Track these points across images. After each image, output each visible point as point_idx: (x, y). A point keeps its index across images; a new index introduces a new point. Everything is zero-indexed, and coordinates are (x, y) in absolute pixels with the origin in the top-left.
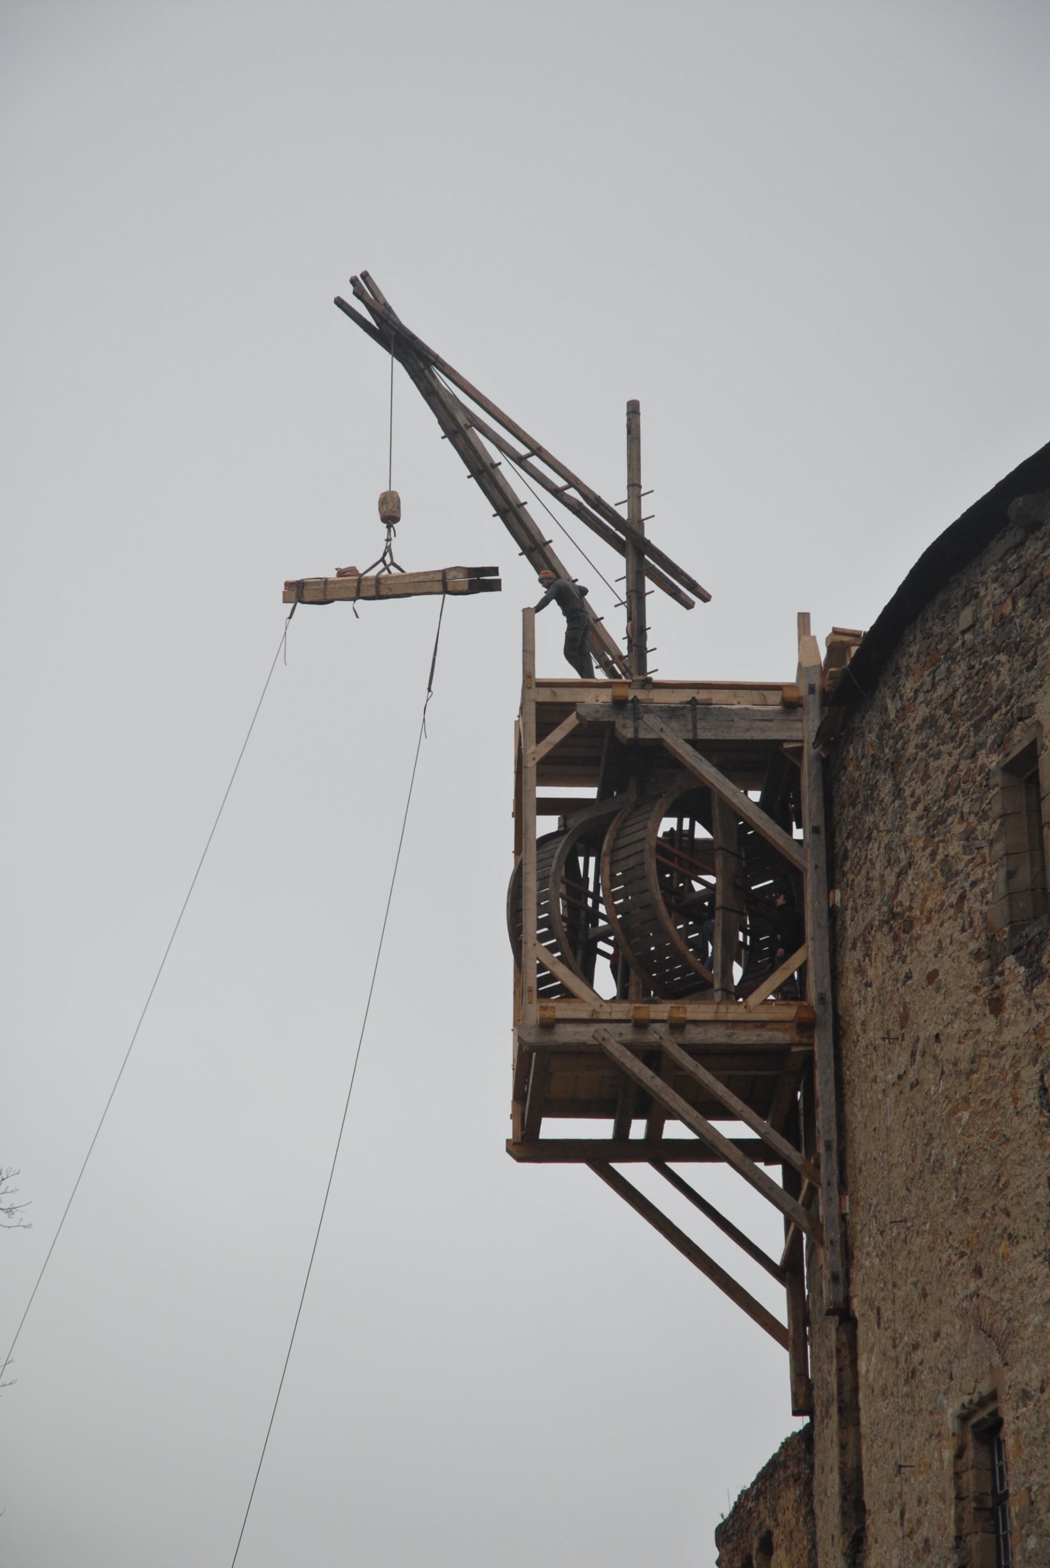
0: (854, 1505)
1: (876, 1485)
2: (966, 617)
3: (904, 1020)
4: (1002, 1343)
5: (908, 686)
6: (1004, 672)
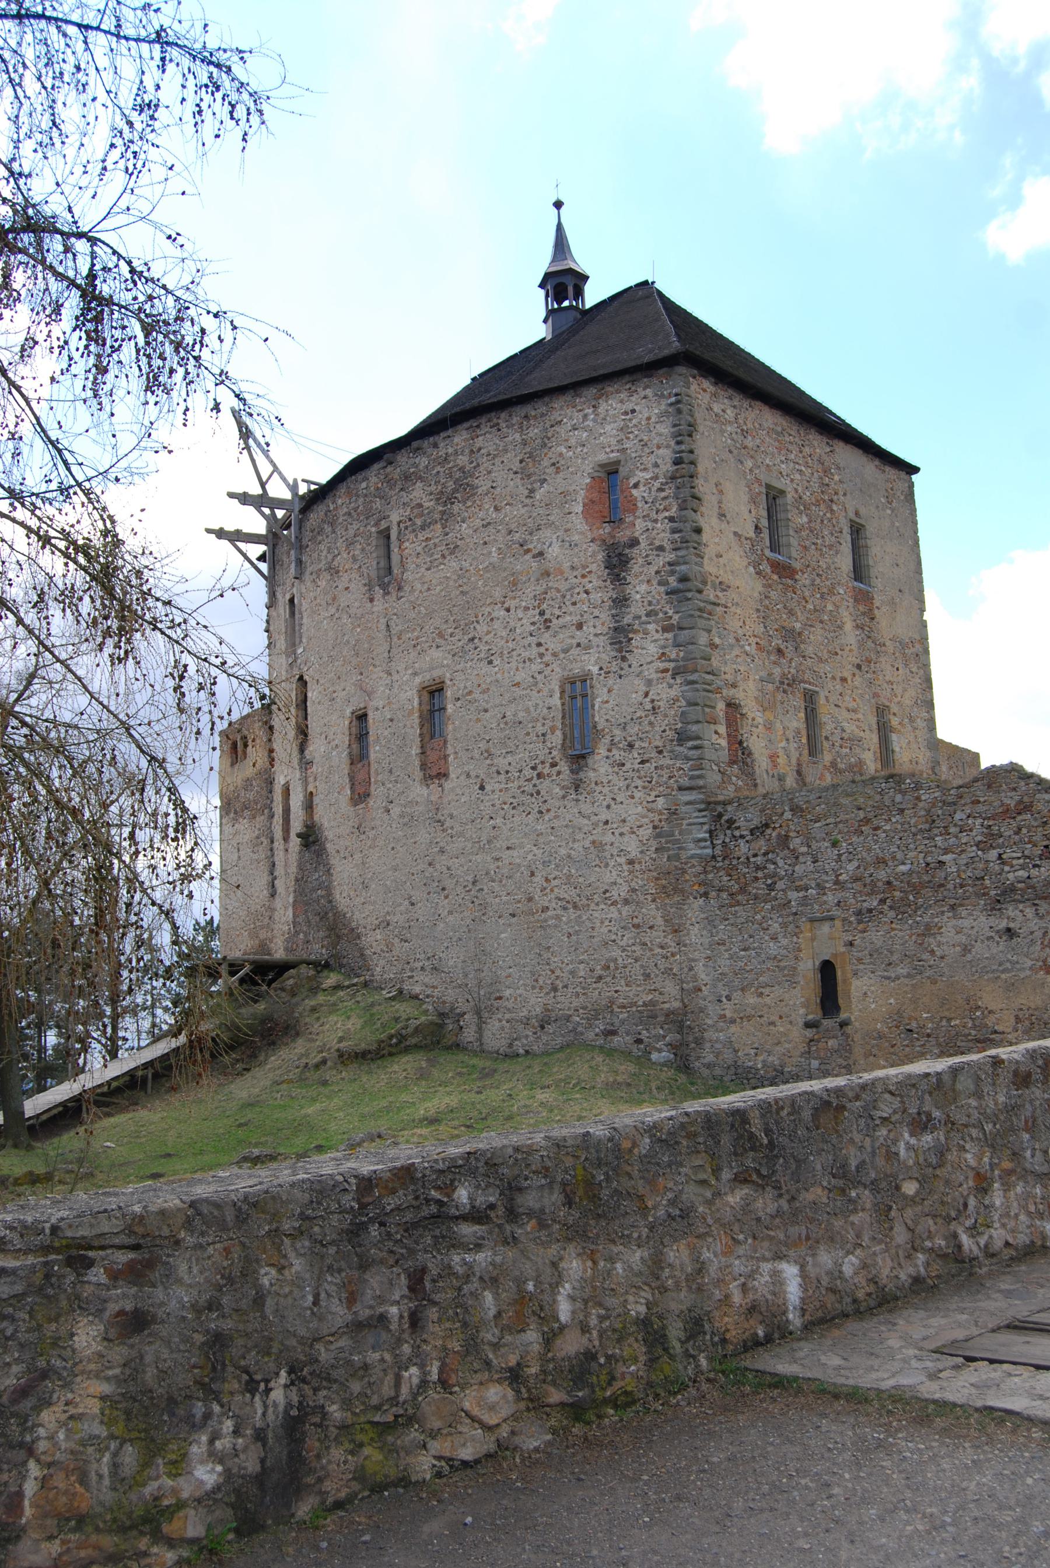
0: (303, 732)
2: (364, 485)
3: (334, 599)
4: (370, 694)
5: (340, 502)
6: (378, 504)
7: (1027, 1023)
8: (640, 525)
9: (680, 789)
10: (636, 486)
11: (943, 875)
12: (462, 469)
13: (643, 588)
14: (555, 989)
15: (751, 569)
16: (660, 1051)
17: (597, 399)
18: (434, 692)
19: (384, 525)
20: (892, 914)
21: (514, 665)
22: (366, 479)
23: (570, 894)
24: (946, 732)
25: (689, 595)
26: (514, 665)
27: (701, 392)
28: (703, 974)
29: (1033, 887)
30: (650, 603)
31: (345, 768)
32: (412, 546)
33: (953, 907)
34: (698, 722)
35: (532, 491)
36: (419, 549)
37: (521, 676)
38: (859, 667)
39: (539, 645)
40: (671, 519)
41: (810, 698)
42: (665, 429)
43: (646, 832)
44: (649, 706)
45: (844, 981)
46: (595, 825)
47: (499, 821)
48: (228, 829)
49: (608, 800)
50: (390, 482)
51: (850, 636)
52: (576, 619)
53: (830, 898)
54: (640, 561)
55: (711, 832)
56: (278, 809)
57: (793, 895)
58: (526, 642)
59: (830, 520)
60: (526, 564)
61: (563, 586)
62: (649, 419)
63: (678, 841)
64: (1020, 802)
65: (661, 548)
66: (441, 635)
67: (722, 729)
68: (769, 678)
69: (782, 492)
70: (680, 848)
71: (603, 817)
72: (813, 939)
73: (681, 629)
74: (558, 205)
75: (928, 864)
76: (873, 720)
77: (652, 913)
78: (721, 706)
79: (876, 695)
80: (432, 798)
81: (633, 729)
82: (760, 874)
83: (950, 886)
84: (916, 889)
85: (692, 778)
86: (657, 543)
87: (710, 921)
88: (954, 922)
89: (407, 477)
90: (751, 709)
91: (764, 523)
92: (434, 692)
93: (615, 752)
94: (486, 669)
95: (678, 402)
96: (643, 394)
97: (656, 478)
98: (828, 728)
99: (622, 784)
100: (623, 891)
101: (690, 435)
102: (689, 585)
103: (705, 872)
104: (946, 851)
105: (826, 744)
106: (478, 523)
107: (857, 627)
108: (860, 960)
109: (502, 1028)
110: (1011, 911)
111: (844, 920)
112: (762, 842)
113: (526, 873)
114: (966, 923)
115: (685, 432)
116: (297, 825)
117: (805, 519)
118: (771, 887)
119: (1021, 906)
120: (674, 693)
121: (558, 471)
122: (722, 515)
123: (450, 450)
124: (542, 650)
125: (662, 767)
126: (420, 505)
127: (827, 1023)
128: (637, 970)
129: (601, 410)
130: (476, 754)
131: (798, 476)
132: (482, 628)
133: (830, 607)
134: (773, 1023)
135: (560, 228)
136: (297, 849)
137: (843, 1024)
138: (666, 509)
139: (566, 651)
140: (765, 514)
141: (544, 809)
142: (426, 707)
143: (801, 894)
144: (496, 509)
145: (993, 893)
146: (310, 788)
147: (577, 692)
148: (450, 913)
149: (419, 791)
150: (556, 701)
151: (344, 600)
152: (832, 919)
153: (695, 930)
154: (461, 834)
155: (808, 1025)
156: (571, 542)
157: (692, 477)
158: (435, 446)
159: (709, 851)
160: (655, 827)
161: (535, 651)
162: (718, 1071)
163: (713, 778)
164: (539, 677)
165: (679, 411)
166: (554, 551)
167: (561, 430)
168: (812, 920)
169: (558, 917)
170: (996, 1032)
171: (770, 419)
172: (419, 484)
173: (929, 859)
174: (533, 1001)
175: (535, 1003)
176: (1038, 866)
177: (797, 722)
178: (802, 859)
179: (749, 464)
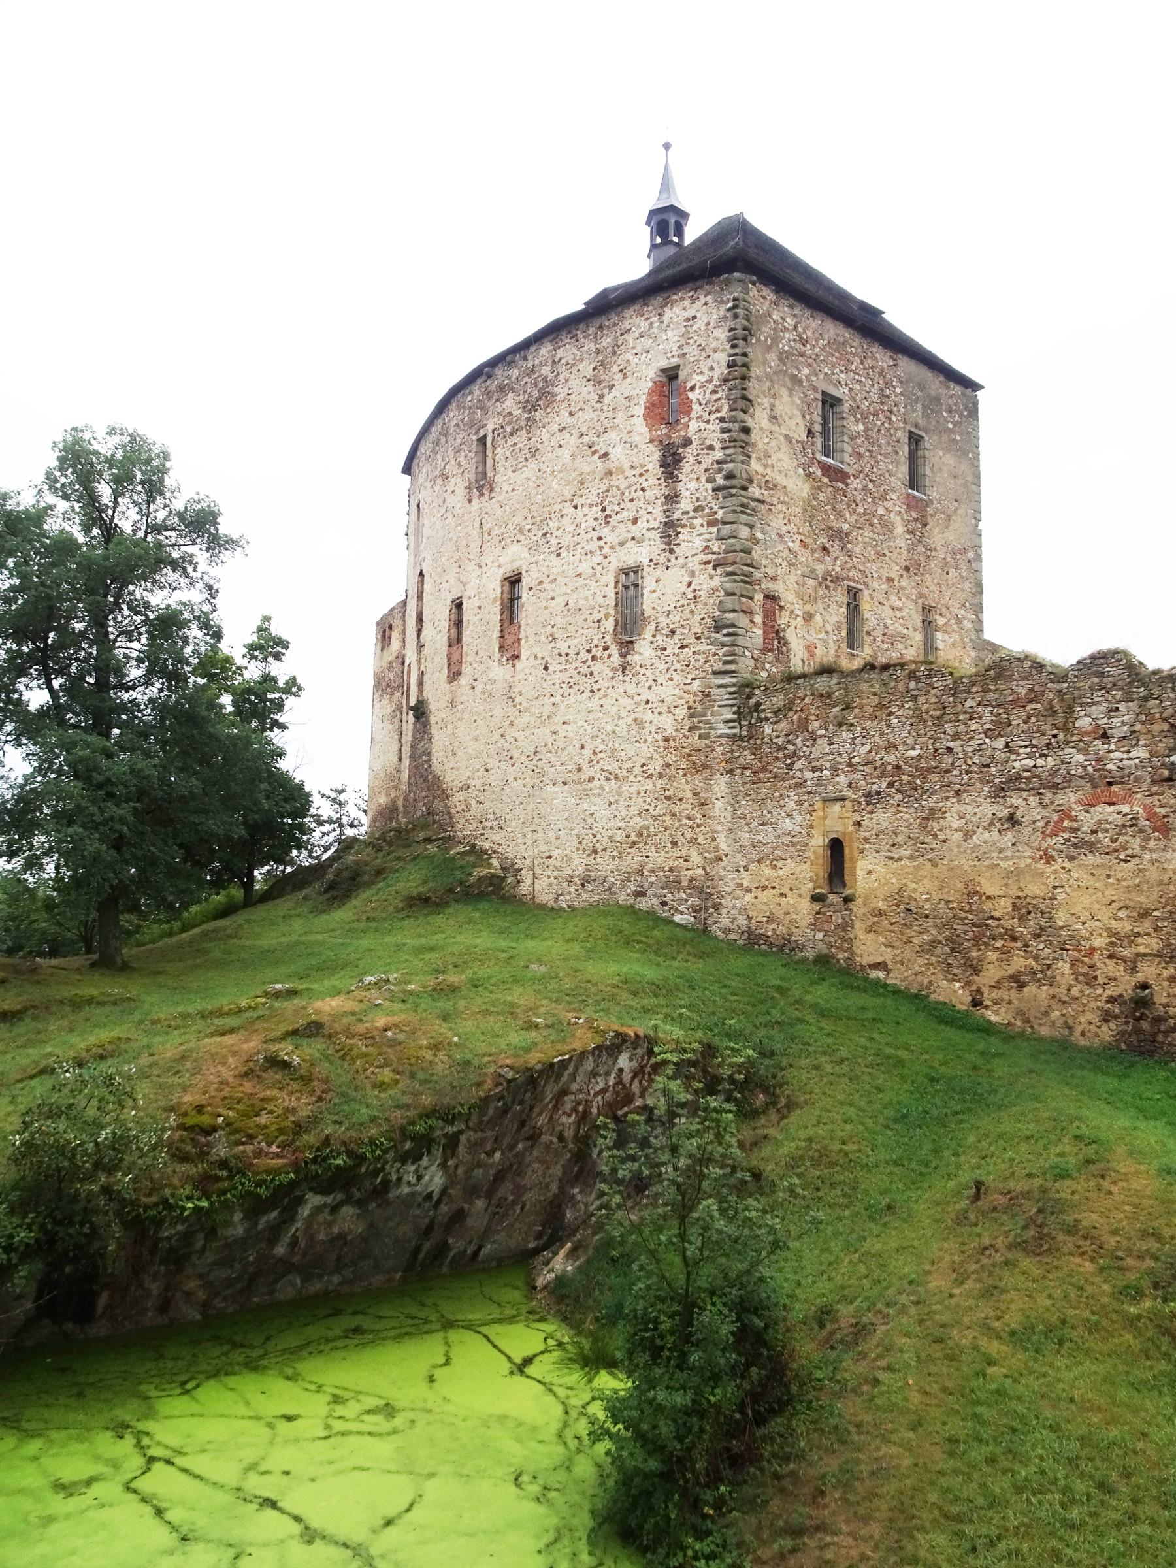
0: (420, 619)
7: (1024, 911)
8: (694, 425)
9: (714, 673)
10: (692, 389)
11: (950, 760)
12: (545, 379)
13: (693, 485)
14: (595, 852)
15: (801, 471)
16: (681, 913)
17: (662, 307)
18: (514, 581)
19: (482, 433)
20: (899, 797)
22: (471, 393)
23: (613, 766)
24: (989, 634)
25: (733, 491)
26: (578, 556)
27: (761, 299)
28: (724, 845)
29: (1038, 776)
30: (698, 499)
31: (444, 649)
32: (501, 451)
33: (957, 793)
34: (734, 611)
35: (601, 396)
36: (508, 454)
37: (585, 568)
38: (907, 569)
39: (600, 538)
40: (722, 420)
41: (853, 595)
42: (722, 334)
43: (682, 712)
44: (691, 596)
45: (854, 861)
47: (558, 699)
49: (651, 682)
52: (632, 515)
53: (843, 779)
54: (692, 459)
55: (738, 713)
57: (808, 775)
58: (588, 536)
59: (888, 430)
61: (623, 484)
62: (708, 324)
63: (708, 722)
64: (1032, 690)
65: (711, 448)
66: (521, 531)
67: (758, 619)
68: (812, 574)
69: (839, 400)
70: (710, 728)
71: (644, 697)
72: (825, 818)
73: (724, 523)
74: (667, 146)
75: (936, 750)
76: (917, 619)
77: (684, 786)
78: (759, 597)
79: (921, 596)
80: (508, 677)
81: (676, 617)
82: (781, 755)
83: (956, 772)
84: (924, 773)
85: (726, 663)
86: (708, 443)
87: (734, 795)
88: (957, 807)
91: (817, 428)
92: (514, 581)
93: (658, 637)
94: (556, 561)
95: (735, 307)
96: (703, 299)
97: (710, 381)
99: (663, 667)
100: (657, 765)
101: (745, 339)
102: (734, 482)
103: (732, 751)
104: (955, 737)
105: (867, 639)
106: (555, 427)
107: (909, 532)
108: (866, 839)
109: (551, 884)
110: (1015, 800)
111: (853, 800)
112: (783, 725)
113: (578, 746)
114: (969, 809)
115: (742, 335)
117: (861, 427)
118: (790, 767)
119: (1025, 794)
120: (716, 582)
121: (625, 377)
123: (537, 362)
124: (601, 543)
125: (699, 653)
126: (510, 414)
127: (832, 898)
128: (666, 838)
129: (666, 319)
130: (543, 639)
131: (857, 387)
132: (553, 524)
133: (881, 511)
135: (666, 168)
138: (718, 411)
139: (621, 544)
140: (819, 419)
141: (595, 688)
142: (507, 596)
143: (817, 774)
144: (571, 414)
145: (997, 780)
148: (516, 779)
149: (499, 672)
152: (843, 799)
153: (719, 804)
154: (527, 710)
156: (634, 443)
157: (744, 378)
159: (736, 731)
160: (690, 708)
162: (732, 936)
163: (745, 665)
164: (599, 568)
167: (629, 338)
168: (824, 801)
169: (602, 788)
170: (992, 918)
171: (834, 330)
172: (511, 395)
173: (938, 745)
174: (577, 861)
175: (579, 864)
176: (1045, 756)
177: (837, 615)
178: (819, 741)
179: (806, 371)
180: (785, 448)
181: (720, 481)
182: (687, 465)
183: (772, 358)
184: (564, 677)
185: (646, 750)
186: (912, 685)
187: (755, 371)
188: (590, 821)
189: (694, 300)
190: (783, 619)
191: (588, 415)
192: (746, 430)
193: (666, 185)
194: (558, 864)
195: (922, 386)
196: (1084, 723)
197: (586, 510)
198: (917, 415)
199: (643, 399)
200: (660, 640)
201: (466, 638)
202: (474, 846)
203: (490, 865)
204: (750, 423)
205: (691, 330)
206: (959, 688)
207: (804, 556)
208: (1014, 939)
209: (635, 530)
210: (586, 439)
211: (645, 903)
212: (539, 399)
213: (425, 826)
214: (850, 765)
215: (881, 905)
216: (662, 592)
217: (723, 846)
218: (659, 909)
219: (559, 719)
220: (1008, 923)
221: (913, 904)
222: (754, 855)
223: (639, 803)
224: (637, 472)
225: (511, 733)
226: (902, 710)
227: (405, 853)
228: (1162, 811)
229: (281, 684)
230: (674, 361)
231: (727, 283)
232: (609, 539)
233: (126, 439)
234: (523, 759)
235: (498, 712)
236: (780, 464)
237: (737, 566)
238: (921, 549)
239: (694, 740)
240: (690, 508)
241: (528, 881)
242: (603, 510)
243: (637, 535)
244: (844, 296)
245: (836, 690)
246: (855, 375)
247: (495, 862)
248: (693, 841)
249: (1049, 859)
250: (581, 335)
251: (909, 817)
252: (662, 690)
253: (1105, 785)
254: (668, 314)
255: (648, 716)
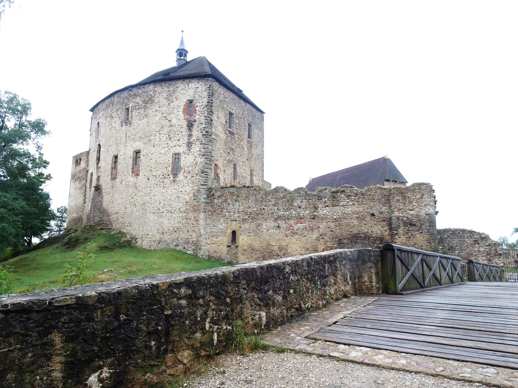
0: (98, 159)
1: (101, 158)
8: (197, 117)
10: (197, 107)
12: (151, 95)
13: (196, 133)
14: (163, 233)
18: (137, 152)
19: (127, 107)
21: (160, 148)
23: (170, 209)
26: (160, 148)
27: (216, 85)
31: (110, 170)
32: (135, 113)
33: (266, 220)
35: (169, 104)
37: (162, 151)
40: (205, 116)
41: (235, 165)
42: (206, 94)
43: (191, 195)
45: (238, 236)
46: (178, 192)
47: (152, 188)
48: (72, 184)
50: (130, 96)
51: (246, 152)
52: (178, 139)
53: (236, 215)
55: (208, 196)
56: (89, 180)
57: (227, 214)
60: (166, 123)
65: (202, 123)
67: (213, 171)
71: (180, 190)
74: (183, 31)
77: (191, 215)
78: (213, 165)
79: (250, 167)
80: (135, 181)
81: (190, 168)
84: (258, 214)
87: (206, 218)
88: (265, 223)
89: (135, 95)
90: (220, 165)
91: (228, 121)
92: (137, 152)
94: (153, 148)
97: (202, 105)
98: (239, 173)
99: (186, 182)
104: (265, 206)
106: (154, 110)
110: (279, 222)
114: (268, 224)
115: (211, 95)
116: (94, 184)
118: (222, 211)
120: (202, 160)
121: (177, 100)
122: (218, 117)
127: (232, 246)
129: (190, 86)
130: (148, 170)
132: (152, 138)
134: (219, 246)
136: (93, 191)
137: (237, 247)
139: (174, 146)
144: (159, 107)
146: (99, 175)
147: (177, 157)
149: (132, 179)
150: (171, 159)
151: (114, 125)
152: (236, 220)
153: (201, 221)
154: (141, 191)
155: (228, 246)
156: (179, 119)
158: (144, 88)
161: (166, 145)
162: (204, 257)
163: (209, 183)
165: (210, 90)
166: (174, 121)
167: (179, 89)
169: (166, 215)
171: (232, 95)
175: (158, 237)
177: (231, 171)
180: (220, 126)
181: (204, 133)
182: (195, 127)
183: (218, 101)
184: (154, 182)
185: (180, 205)
186: (255, 192)
187: (214, 105)
188: (162, 224)
189: (198, 83)
190: (219, 171)
191: (165, 108)
192: (212, 120)
193: (182, 42)
194: (151, 237)
195: (252, 112)
196: (295, 204)
197: (163, 135)
198: (250, 119)
199: (182, 107)
200: (185, 174)
201: (119, 167)
202: (120, 231)
203: (127, 237)
204: (212, 119)
205: (195, 90)
206: (267, 194)
207: (224, 155)
208: (278, 256)
209: (179, 143)
210: (164, 115)
211: (178, 248)
212: (148, 101)
213: (99, 225)
214: (238, 211)
215: (246, 248)
216: (186, 161)
217: (202, 232)
218: (183, 250)
219: (152, 194)
220: (277, 252)
221: (254, 248)
222: (211, 235)
223: (178, 220)
224: (180, 127)
225: (135, 198)
226: (252, 198)
227: (94, 233)
228: (312, 225)
229: (45, 176)
230: (192, 98)
231: (208, 80)
232: (171, 144)
233: (12, 96)
234: (139, 205)
235: (131, 191)
236: (219, 130)
237: (208, 156)
238: (250, 154)
239: (195, 203)
240: (195, 139)
241: (140, 242)
242: (169, 136)
243: (180, 145)
244: (222, 75)
245: (235, 191)
246: (236, 107)
247: (128, 236)
248: (194, 231)
249: (287, 236)
250: (163, 85)
251: (253, 225)
252: (186, 188)
253: (300, 219)
254: (190, 85)
255: (181, 195)
